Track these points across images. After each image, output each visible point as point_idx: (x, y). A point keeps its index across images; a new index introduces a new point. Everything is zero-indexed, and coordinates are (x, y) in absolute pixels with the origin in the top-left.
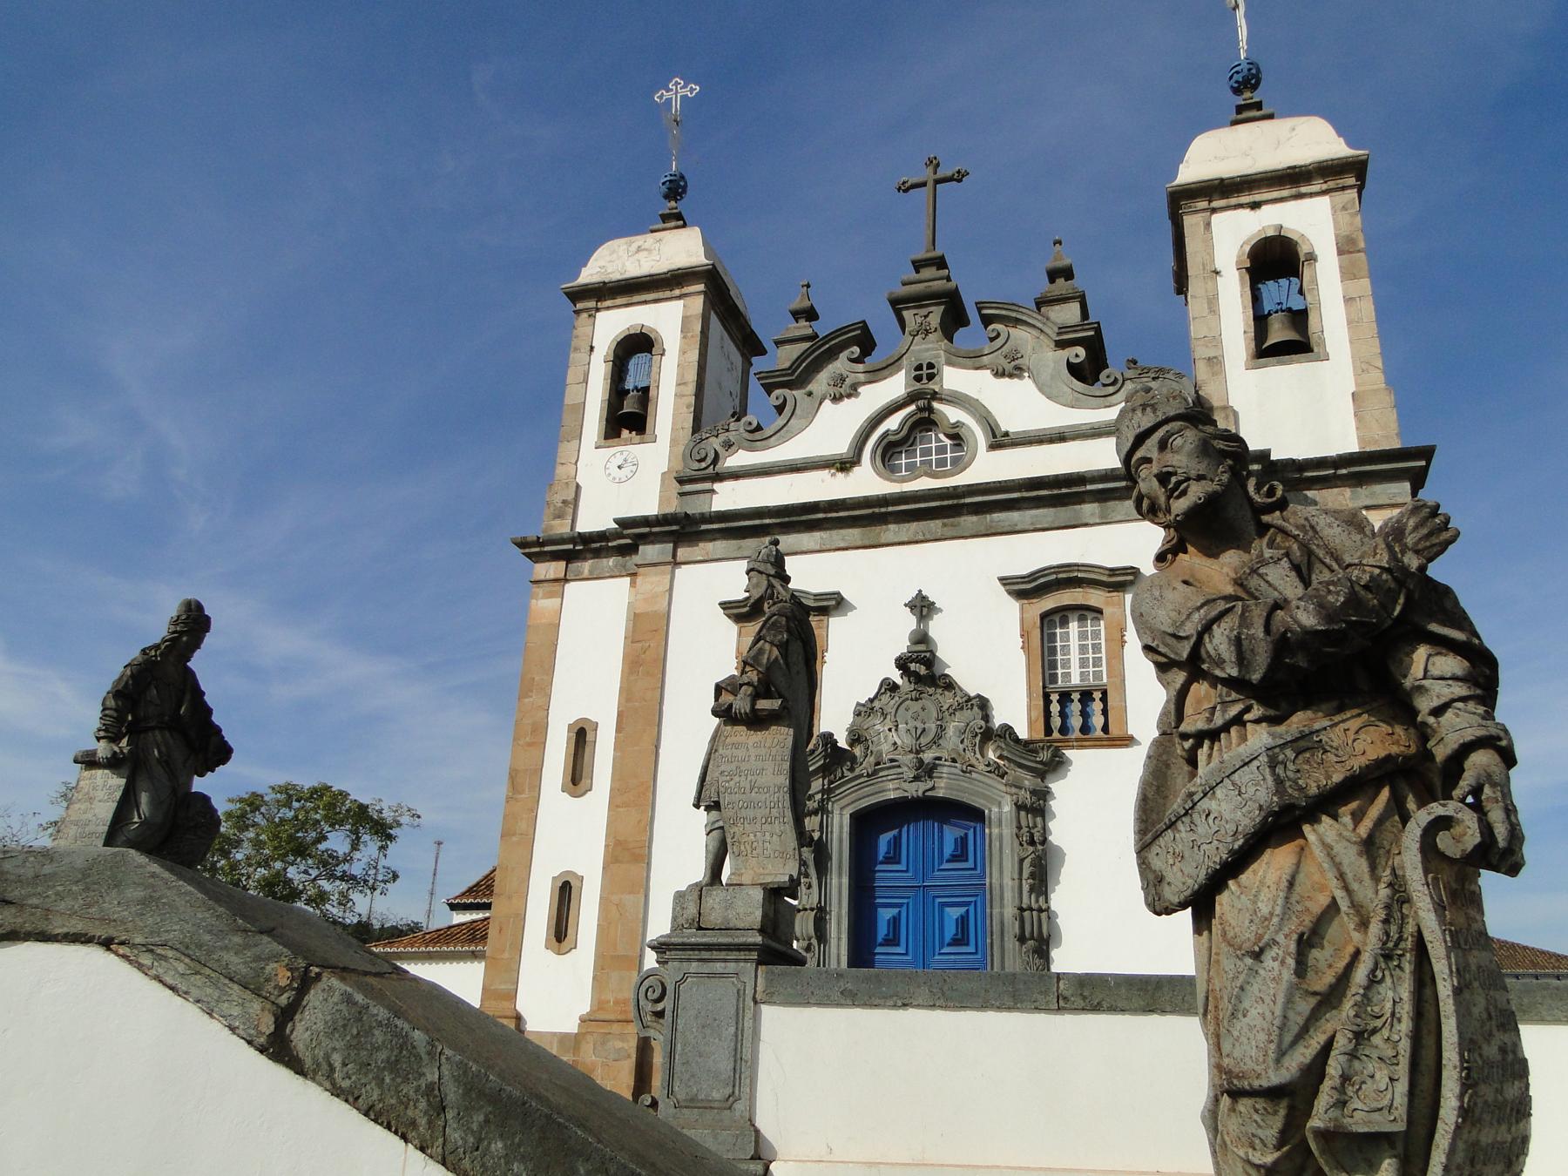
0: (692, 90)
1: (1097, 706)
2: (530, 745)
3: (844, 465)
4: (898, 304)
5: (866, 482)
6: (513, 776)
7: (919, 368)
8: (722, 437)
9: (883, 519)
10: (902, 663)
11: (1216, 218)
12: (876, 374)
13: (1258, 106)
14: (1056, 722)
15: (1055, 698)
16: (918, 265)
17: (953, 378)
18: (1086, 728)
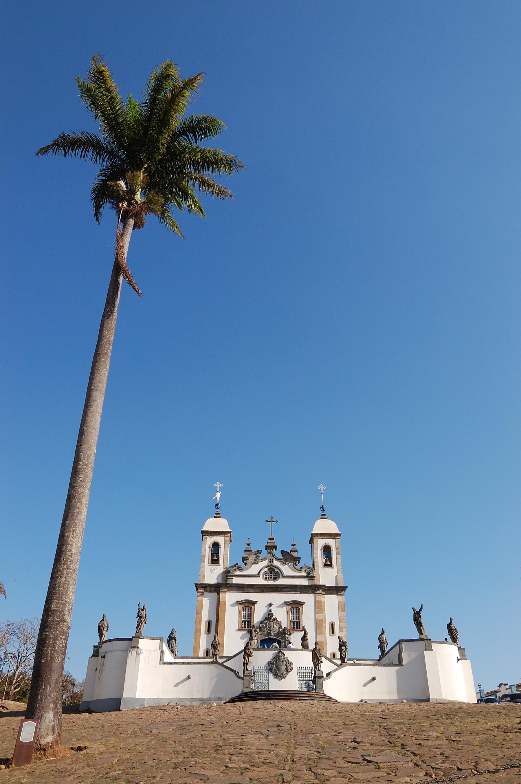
0: (221, 485)
1: (298, 624)
2: (199, 624)
3: (258, 576)
4: (266, 546)
5: (261, 581)
6: (196, 630)
7: (270, 560)
8: (234, 568)
9: (264, 588)
10: (269, 615)
11: (318, 539)
12: (263, 560)
13: (325, 515)
14: (292, 626)
15: (292, 623)
16: (270, 539)
17: (276, 563)
18: (297, 628)
